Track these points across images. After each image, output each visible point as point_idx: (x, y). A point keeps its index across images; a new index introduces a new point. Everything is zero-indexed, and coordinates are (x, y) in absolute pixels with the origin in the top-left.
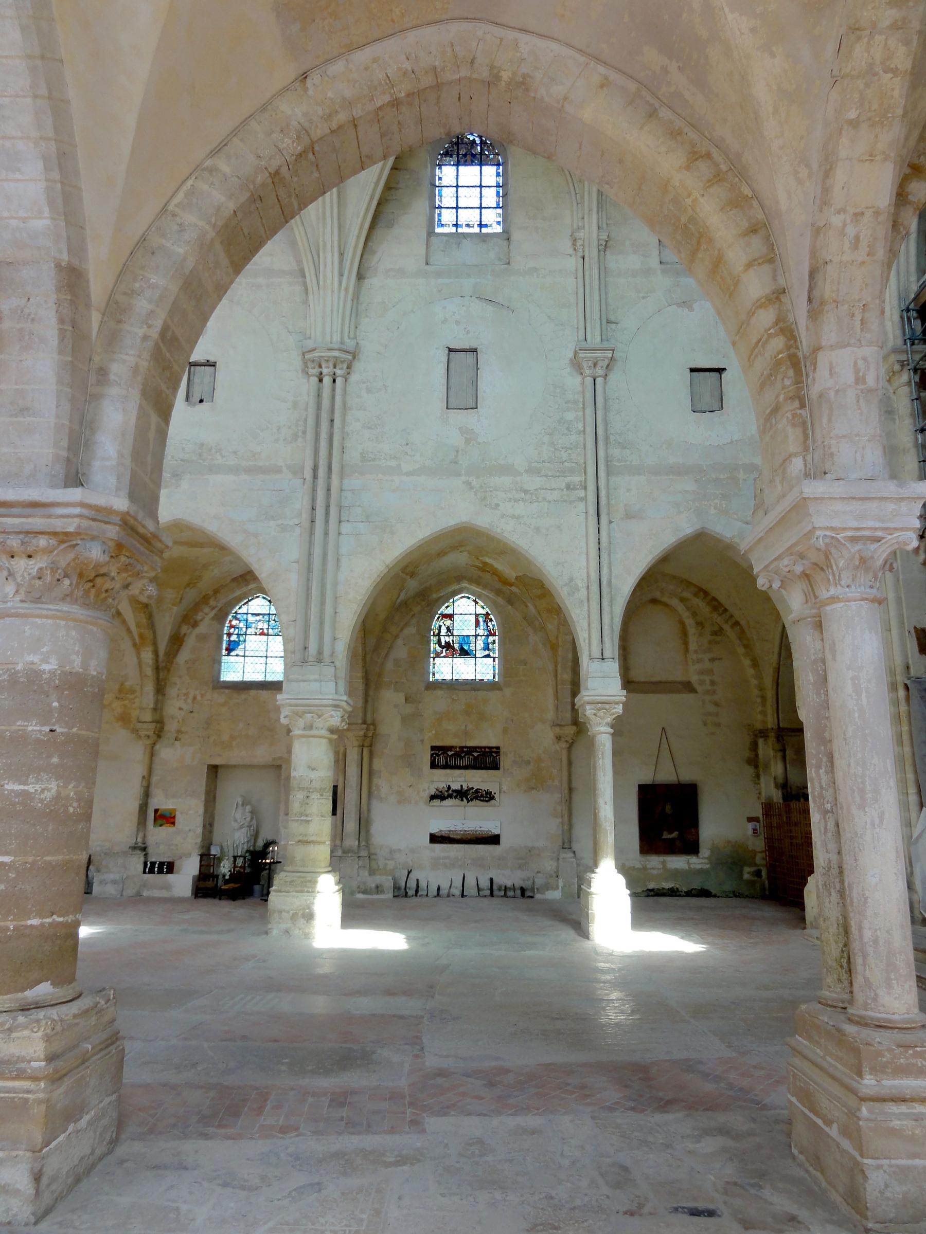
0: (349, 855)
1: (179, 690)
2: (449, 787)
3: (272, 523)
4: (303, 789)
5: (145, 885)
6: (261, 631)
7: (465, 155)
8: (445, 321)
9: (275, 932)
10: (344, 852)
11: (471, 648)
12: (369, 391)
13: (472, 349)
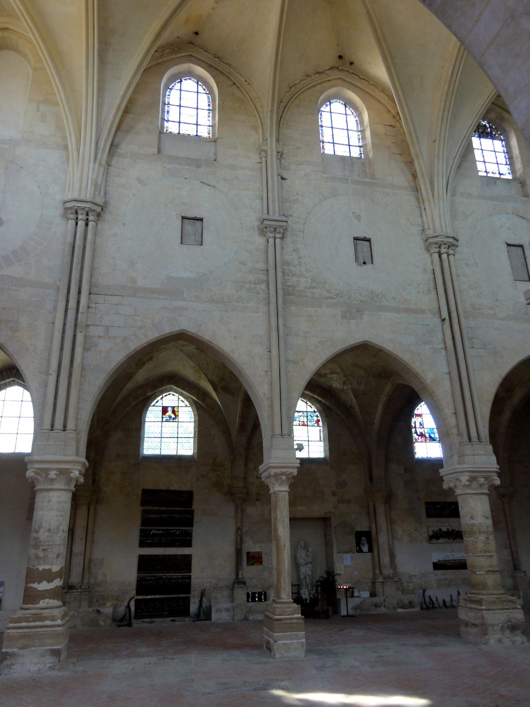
0: (389, 580)
1: (255, 464)
2: (440, 530)
3: (427, 347)
4: (484, 532)
5: (250, 611)
6: (303, 423)
7: (482, 133)
8: (501, 227)
9: (492, 641)
10: (385, 578)
11: (436, 436)
12: (467, 265)
13: (520, 245)
